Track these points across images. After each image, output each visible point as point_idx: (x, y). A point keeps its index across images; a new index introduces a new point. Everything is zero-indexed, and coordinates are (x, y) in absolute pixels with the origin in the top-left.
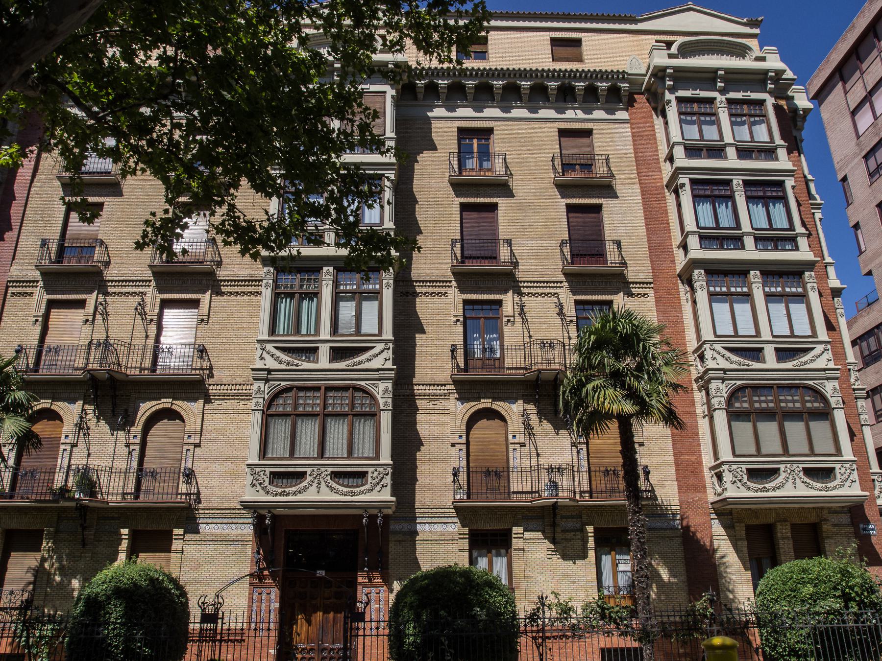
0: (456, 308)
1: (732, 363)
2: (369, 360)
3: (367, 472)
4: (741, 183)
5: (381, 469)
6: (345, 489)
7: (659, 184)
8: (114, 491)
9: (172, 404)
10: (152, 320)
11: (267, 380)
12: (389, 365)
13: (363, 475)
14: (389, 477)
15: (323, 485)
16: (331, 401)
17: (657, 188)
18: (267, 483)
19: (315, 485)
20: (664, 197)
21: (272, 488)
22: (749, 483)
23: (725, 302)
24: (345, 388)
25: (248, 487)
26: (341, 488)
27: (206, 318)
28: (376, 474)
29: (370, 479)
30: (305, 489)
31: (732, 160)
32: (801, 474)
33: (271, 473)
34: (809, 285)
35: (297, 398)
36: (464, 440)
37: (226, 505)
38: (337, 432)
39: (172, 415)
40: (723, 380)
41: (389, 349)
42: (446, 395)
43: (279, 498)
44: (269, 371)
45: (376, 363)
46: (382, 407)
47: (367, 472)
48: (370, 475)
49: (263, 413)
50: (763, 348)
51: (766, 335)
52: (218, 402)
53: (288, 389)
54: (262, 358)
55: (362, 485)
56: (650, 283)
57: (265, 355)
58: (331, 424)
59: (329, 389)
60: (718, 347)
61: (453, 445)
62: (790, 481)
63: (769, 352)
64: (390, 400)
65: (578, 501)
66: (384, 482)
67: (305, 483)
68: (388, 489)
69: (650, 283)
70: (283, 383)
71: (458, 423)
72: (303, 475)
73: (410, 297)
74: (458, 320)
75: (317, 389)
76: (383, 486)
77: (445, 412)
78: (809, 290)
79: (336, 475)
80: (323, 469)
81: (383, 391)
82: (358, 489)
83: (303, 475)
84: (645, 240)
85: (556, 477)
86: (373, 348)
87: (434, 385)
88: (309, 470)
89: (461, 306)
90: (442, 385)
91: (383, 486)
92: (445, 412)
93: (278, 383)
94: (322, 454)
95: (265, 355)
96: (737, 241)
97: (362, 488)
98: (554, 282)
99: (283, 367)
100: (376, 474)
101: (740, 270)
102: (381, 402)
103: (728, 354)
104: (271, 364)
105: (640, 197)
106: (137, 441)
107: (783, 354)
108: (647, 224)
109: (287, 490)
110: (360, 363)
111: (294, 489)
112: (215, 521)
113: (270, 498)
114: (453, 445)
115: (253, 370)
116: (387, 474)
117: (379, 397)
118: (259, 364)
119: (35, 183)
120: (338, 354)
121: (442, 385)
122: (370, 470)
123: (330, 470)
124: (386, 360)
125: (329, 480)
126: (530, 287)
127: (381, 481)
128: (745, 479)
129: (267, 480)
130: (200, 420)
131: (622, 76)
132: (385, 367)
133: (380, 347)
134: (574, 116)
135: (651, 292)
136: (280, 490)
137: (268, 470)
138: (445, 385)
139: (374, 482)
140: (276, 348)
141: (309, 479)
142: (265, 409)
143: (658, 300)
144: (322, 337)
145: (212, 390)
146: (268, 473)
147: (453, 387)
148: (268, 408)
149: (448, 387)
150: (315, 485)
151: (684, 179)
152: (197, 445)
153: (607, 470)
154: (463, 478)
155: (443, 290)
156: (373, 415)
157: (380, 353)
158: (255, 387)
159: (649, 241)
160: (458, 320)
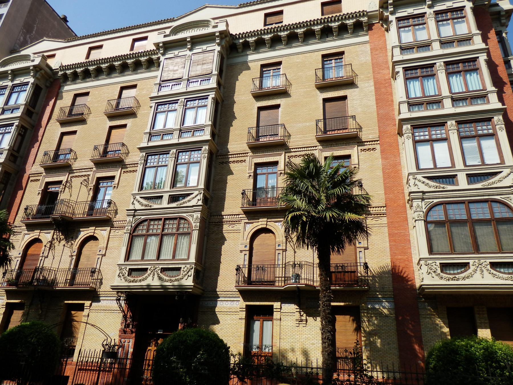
0: (250, 169)
1: (430, 187)
2: (189, 201)
3: (181, 268)
4: (442, 64)
5: (188, 266)
6: (167, 278)
7: (387, 77)
8: (62, 282)
10: (91, 189)
11: (134, 216)
12: (200, 203)
13: (179, 269)
14: (193, 270)
15: (156, 276)
16: (167, 226)
17: (385, 80)
18: (126, 275)
19: (151, 275)
20: (391, 85)
21: (129, 278)
22: (442, 274)
23: (427, 145)
24: (175, 219)
25: (117, 277)
26: (165, 277)
27: (116, 186)
28: (186, 268)
29: (182, 272)
30: (146, 278)
31: (436, 49)
32: (489, 267)
33: (130, 269)
34: (497, 127)
35: (149, 226)
36: (248, 248)
38: (169, 243)
39: (93, 238)
40: (423, 199)
41: (200, 194)
43: (131, 284)
45: (194, 202)
46: (194, 229)
47: (181, 268)
48: (182, 269)
49: (130, 234)
50: (457, 175)
51: (459, 165)
52: (117, 231)
53: (145, 220)
54: (133, 203)
55: (178, 276)
56: (377, 141)
57: (135, 202)
58: (165, 238)
59: (166, 219)
60: (419, 177)
61: (241, 251)
62: (478, 272)
63: (462, 178)
64: (198, 224)
65: (315, 287)
66: (189, 274)
67: (147, 275)
68: (191, 278)
69: (377, 141)
70: (143, 217)
71: (245, 238)
72: (146, 270)
73: (225, 164)
74: (250, 176)
75: (160, 219)
76: (189, 276)
77: (238, 231)
78: (498, 130)
79: (163, 270)
80: (157, 266)
81: (194, 219)
82: (174, 278)
83: (146, 270)
84: (375, 114)
85: (297, 270)
86: (192, 194)
87: (232, 215)
88: (149, 267)
89: (253, 167)
90: (237, 215)
91: (189, 276)
92: (238, 231)
93: (140, 217)
94: (158, 258)
95: (135, 202)
96: (438, 102)
97: (177, 278)
98: (311, 147)
99: (143, 208)
100: (186, 268)
101: (439, 122)
102: (194, 224)
103: (427, 181)
104: (138, 206)
105: (373, 88)
106: (75, 254)
107: (472, 178)
108: (377, 103)
109: (136, 279)
110: (184, 203)
111: (140, 278)
113: (127, 284)
114: (241, 251)
115: (127, 210)
116: (192, 269)
118: (131, 207)
119: (49, 125)
120: (173, 199)
121: (237, 215)
122: (183, 266)
124: (198, 200)
125: (160, 273)
126: (296, 151)
127: (188, 273)
128: (439, 271)
129: (127, 273)
130: (106, 242)
131: (364, 13)
132: (198, 204)
133: (196, 193)
134: (331, 45)
135: (378, 147)
136: (132, 279)
138: (239, 215)
139: (184, 273)
140: (141, 197)
141: (149, 272)
142: (132, 232)
143: (382, 152)
145: (116, 224)
146: (128, 269)
147: (244, 216)
148: (134, 232)
149: (240, 216)
150: (151, 275)
151: (399, 69)
152: (104, 255)
153: (337, 266)
154: (246, 271)
155: (243, 159)
156: (189, 234)
157: (196, 197)
158: (128, 219)
159: (378, 114)
160: (250, 176)
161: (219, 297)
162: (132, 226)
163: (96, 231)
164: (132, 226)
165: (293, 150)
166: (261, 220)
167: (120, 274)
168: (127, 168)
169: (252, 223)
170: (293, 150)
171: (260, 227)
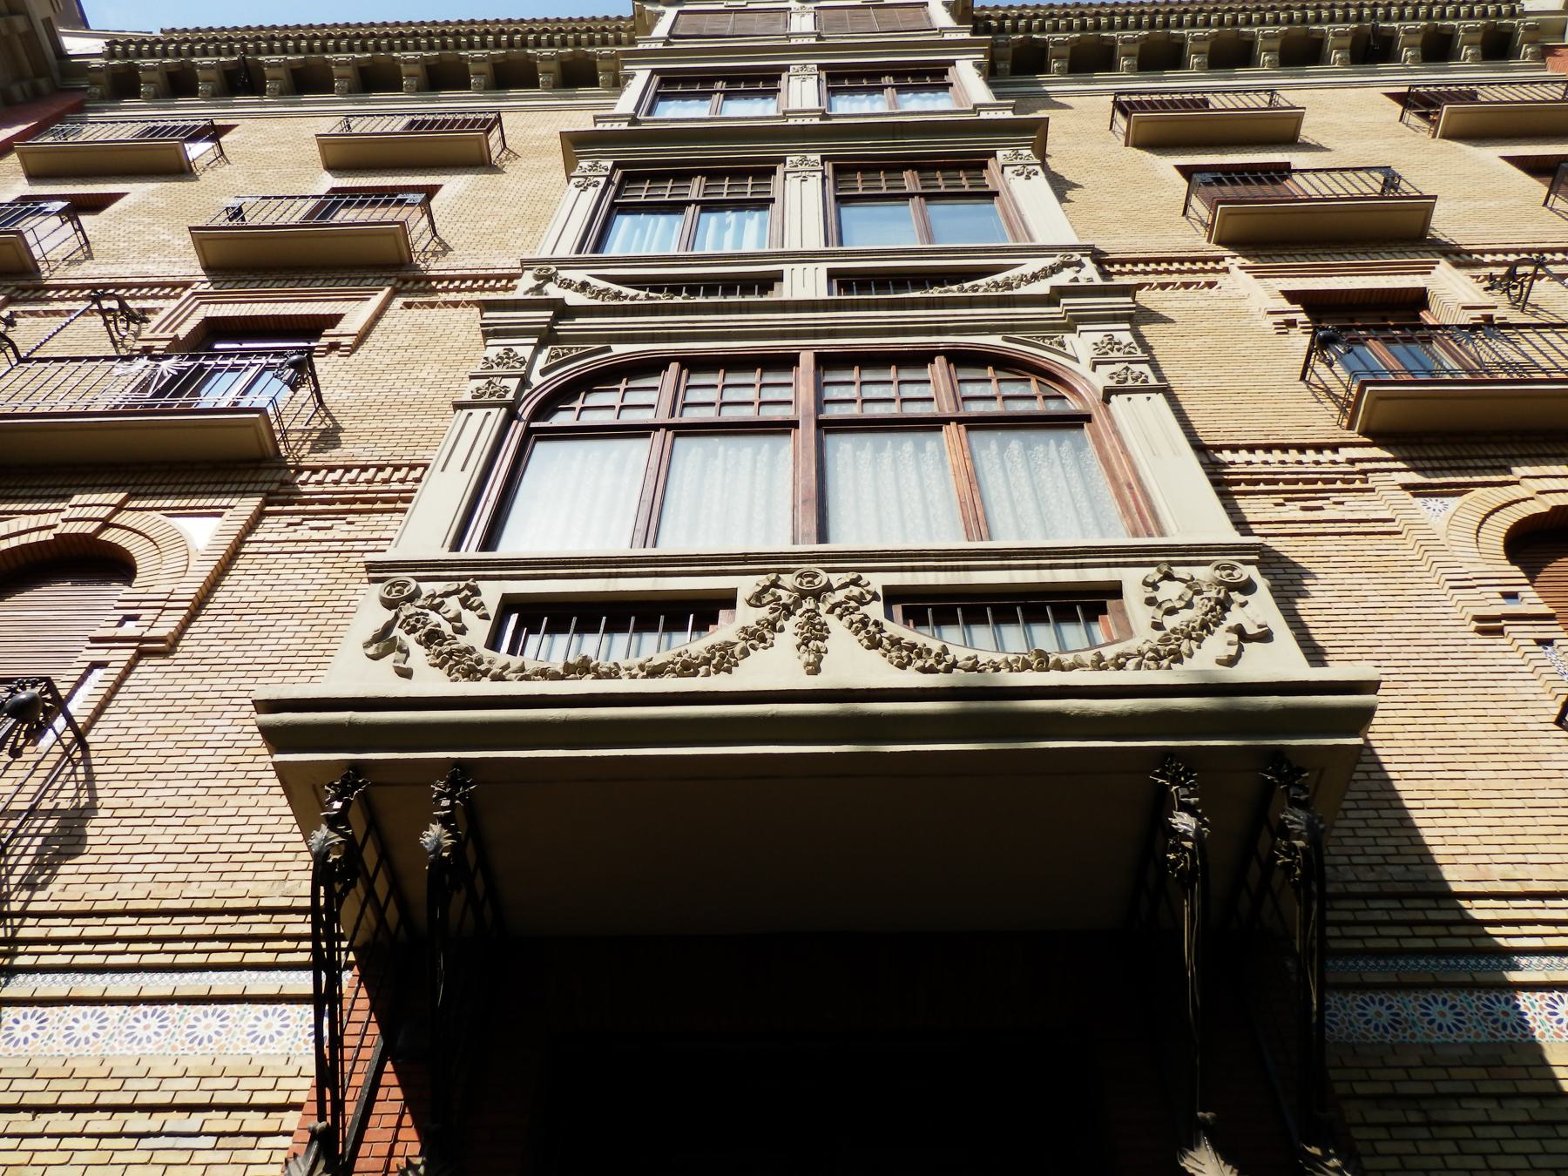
3: (1115, 590)
9: (106, 524)
11: (547, 337)
30: (724, 659)
37: (204, 891)
42: (1355, 481)
44: (563, 311)
47: (1115, 590)
61: (1490, 626)
80: (836, 580)
88: (746, 586)
112: (91, 985)
114: (1490, 626)
117: (1083, 368)
122: (1132, 579)
123: (877, 581)
137: (492, 593)
138: (1335, 448)
142: (525, 411)
144: (792, 245)
145: (309, 484)
160: (1292, 324)
161: (1508, 956)
162: (525, 382)
163: (123, 518)
164: (525, 382)
165: (1488, 258)
166: (1518, 471)
167: (398, 632)
168: (434, 291)
169: (1460, 490)
170: (1488, 258)
171: (1541, 506)
